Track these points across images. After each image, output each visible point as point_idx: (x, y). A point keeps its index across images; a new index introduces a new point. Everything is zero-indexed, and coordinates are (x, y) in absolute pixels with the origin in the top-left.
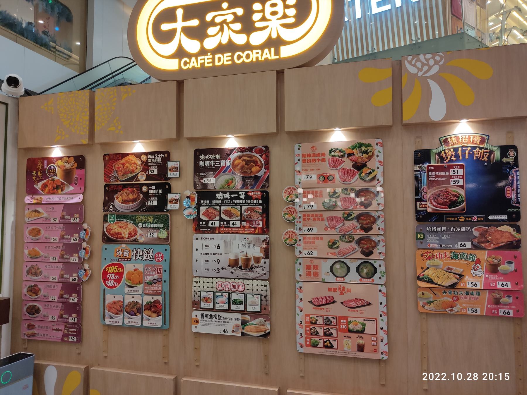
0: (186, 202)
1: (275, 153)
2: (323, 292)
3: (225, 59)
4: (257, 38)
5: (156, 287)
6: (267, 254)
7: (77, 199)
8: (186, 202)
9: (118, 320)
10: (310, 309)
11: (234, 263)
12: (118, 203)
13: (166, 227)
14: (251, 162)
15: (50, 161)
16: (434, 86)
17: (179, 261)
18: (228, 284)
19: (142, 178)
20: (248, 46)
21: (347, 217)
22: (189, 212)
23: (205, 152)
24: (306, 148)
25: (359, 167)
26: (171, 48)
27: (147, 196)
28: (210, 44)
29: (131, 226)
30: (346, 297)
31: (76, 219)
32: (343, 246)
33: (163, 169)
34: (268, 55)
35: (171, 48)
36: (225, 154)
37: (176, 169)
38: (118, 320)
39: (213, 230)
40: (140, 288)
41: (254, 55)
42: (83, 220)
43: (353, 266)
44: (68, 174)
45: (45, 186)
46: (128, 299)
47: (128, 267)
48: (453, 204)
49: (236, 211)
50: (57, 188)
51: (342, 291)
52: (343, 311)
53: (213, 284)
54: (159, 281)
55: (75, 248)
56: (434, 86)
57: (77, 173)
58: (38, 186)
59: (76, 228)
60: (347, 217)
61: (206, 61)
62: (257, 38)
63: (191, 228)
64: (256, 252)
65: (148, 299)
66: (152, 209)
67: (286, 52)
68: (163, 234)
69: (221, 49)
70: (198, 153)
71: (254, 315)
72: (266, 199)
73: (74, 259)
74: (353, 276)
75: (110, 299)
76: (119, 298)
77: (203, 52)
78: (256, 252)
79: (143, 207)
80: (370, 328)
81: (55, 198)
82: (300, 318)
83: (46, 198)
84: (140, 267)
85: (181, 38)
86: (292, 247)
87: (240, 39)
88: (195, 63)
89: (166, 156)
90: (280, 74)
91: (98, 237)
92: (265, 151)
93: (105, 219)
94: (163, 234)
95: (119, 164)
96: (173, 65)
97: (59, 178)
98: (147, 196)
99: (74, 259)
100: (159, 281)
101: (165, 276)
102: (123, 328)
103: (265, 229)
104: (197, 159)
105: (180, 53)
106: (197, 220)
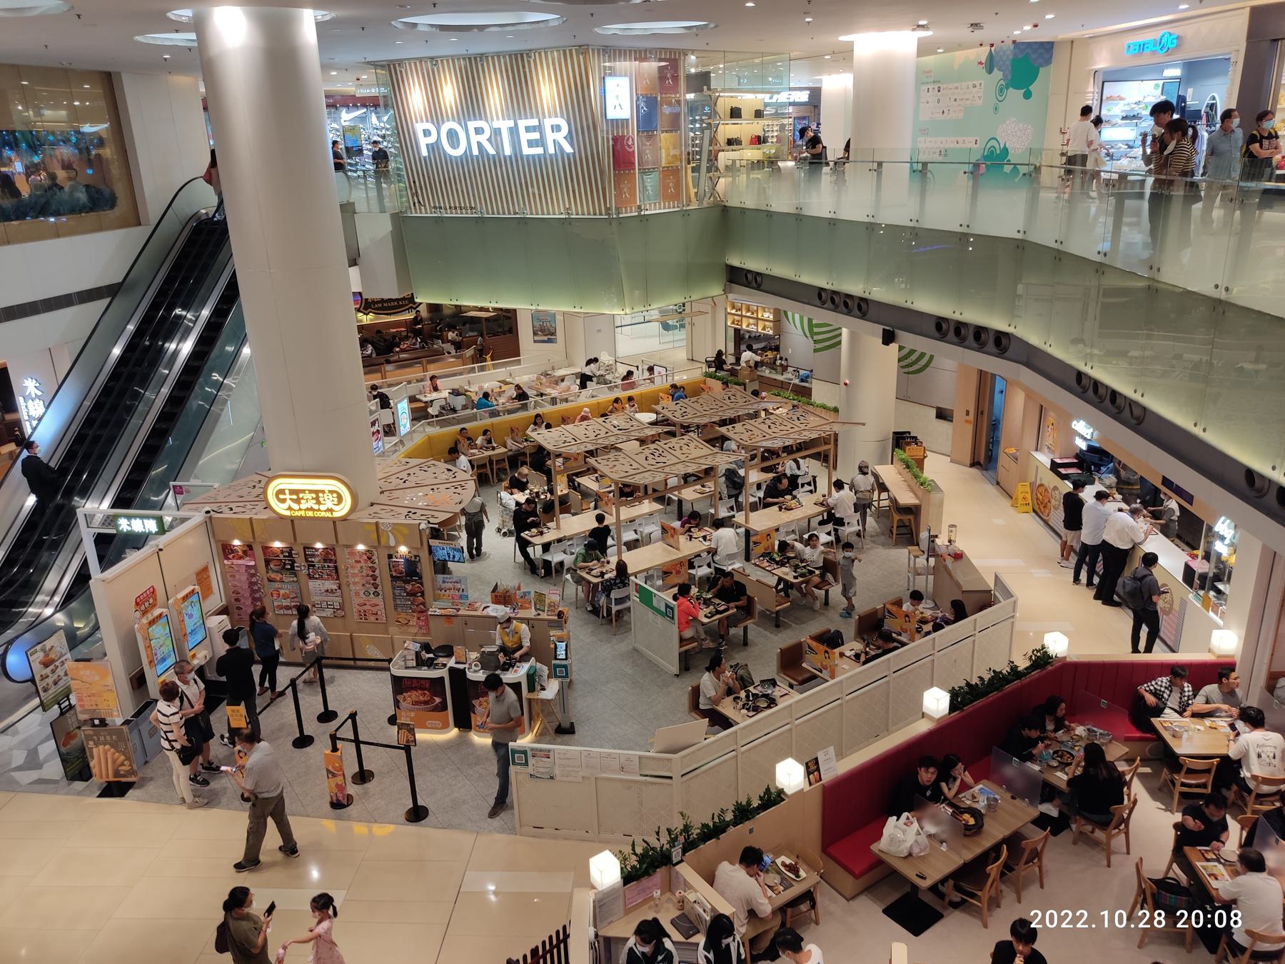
0: (303, 568)
1: (337, 550)
2: (362, 601)
3: (310, 514)
4: (323, 508)
5: (295, 599)
6: (339, 588)
7: (252, 563)
8: (303, 568)
9: (282, 612)
10: (358, 607)
11: (327, 591)
12: (272, 566)
13: (296, 576)
14: (328, 553)
15: (234, 546)
16: (390, 534)
17: (304, 590)
18: (326, 599)
19: (281, 557)
20: (319, 510)
21: (368, 576)
22: (305, 571)
23: (308, 548)
24: (349, 550)
25: (370, 558)
26: (286, 506)
27: (285, 564)
28: (303, 506)
29: (280, 575)
30: (370, 603)
31: (253, 571)
32: (367, 585)
33: (290, 555)
34: (328, 515)
35: (286, 506)
36: (317, 550)
37: (298, 567)
38: (282, 612)
39: (316, 578)
40: (289, 600)
41: (323, 514)
42: (256, 571)
43: (372, 593)
44: (244, 552)
45: (234, 557)
46: (284, 604)
47: (282, 592)
48: (401, 573)
49: (324, 572)
50: (240, 558)
51: (368, 601)
52: (370, 608)
53: (319, 598)
54: (296, 597)
55: (256, 583)
56: (390, 534)
57: (249, 552)
58: (231, 556)
59: (253, 575)
60: (368, 576)
61: (303, 513)
62: (323, 508)
63: (307, 577)
64: (335, 587)
65: (293, 604)
66: (288, 569)
67: (336, 515)
68: (295, 579)
69: (308, 509)
70: (305, 548)
71: (338, 609)
72: (336, 568)
73: (256, 588)
74: (372, 596)
75: (276, 604)
76: (280, 603)
77: (300, 509)
78: (335, 587)
79: (283, 568)
80: (379, 613)
81: (240, 562)
82: (355, 610)
83: (235, 562)
84: (287, 592)
85: (289, 502)
86: (349, 585)
87: (316, 507)
88: (298, 514)
89: (291, 549)
90: (334, 522)
91: (266, 580)
92: (333, 549)
93: (267, 572)
94: (295, 579)
95: (269, 550)
96: (288, 513)
97: (240, 553)
98: (285, 564)
99: (256, 588)
100: (296, 597)
101: (299, 595)
102: (284, 614)
103: (338, 579)
104: (305, 551)
105: (290, 508)
106: (309, 574)
